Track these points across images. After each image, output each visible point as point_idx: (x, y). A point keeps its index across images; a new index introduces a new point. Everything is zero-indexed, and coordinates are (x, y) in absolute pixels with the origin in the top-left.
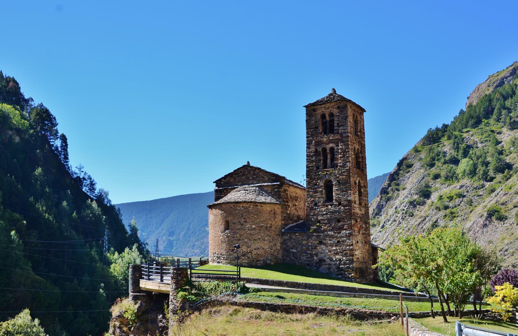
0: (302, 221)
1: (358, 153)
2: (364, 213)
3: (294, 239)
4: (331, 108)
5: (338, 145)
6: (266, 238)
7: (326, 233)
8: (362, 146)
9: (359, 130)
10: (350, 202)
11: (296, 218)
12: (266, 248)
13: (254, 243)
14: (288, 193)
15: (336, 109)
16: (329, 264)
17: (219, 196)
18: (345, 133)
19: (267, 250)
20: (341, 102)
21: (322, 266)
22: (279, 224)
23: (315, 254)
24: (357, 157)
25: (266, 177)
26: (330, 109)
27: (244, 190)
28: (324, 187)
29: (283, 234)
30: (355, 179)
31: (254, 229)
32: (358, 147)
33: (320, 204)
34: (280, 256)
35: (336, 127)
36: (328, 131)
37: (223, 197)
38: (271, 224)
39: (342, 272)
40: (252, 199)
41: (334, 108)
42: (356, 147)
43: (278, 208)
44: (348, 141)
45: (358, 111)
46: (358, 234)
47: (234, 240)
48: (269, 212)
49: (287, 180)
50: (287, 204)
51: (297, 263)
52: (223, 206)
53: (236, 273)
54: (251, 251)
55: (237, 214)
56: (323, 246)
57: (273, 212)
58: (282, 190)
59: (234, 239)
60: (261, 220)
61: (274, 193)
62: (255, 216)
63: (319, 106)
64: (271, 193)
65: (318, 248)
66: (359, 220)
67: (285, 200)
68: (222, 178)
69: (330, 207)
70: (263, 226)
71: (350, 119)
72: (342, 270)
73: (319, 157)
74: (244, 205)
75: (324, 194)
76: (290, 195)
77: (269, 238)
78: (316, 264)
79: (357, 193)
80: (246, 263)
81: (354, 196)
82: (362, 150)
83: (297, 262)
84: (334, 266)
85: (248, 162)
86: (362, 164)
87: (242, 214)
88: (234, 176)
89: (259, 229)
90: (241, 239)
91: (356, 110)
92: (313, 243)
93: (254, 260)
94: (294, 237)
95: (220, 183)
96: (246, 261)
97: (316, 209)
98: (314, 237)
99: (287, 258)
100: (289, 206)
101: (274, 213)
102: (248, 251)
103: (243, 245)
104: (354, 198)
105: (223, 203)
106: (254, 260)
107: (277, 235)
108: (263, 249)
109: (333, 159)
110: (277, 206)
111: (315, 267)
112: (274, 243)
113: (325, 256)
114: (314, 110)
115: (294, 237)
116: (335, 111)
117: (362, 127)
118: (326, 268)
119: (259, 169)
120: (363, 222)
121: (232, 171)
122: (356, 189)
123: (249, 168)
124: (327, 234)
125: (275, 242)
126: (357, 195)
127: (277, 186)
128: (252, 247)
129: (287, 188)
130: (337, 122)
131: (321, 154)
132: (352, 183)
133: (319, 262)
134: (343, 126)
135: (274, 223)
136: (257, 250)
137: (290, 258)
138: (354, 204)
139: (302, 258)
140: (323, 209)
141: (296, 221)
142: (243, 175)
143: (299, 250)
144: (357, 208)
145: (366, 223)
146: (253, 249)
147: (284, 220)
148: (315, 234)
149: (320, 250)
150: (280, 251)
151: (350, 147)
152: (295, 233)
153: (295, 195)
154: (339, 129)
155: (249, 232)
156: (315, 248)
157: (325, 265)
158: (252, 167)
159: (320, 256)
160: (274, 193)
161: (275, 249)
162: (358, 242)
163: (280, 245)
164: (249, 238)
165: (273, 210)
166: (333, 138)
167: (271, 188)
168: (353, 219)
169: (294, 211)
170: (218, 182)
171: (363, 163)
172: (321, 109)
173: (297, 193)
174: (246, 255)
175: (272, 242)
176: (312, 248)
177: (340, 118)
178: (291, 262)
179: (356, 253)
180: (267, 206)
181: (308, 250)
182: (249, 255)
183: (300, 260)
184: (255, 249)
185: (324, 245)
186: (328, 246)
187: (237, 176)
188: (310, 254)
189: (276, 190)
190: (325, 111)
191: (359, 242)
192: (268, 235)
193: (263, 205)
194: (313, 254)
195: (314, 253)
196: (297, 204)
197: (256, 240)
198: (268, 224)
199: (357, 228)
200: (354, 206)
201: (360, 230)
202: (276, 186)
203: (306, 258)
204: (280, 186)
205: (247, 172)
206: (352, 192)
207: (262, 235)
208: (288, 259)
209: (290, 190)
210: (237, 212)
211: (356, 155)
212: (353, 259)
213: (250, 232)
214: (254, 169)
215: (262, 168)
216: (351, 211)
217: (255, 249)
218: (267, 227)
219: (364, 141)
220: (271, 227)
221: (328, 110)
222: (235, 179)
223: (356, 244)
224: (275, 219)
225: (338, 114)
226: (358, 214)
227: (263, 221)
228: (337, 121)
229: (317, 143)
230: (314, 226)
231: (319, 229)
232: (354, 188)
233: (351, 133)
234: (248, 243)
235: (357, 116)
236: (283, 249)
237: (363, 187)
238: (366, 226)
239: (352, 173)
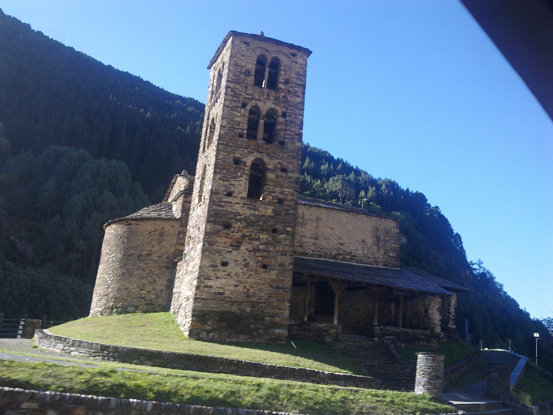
6: (136, 273)
19: (134, 290)
30: (238, 155)
48: (150, 232)
70: (133, 254)
77: (142, 272)
125: (153, 278)
175: (147, 278)
180: (149, 223)
192: (140, 267)
193: (138, 223)
198: (144, 250)
207: (130, 267)
218: (141, 255)
220: (148, 255)
224: (160, 243)
227: (135, 246)
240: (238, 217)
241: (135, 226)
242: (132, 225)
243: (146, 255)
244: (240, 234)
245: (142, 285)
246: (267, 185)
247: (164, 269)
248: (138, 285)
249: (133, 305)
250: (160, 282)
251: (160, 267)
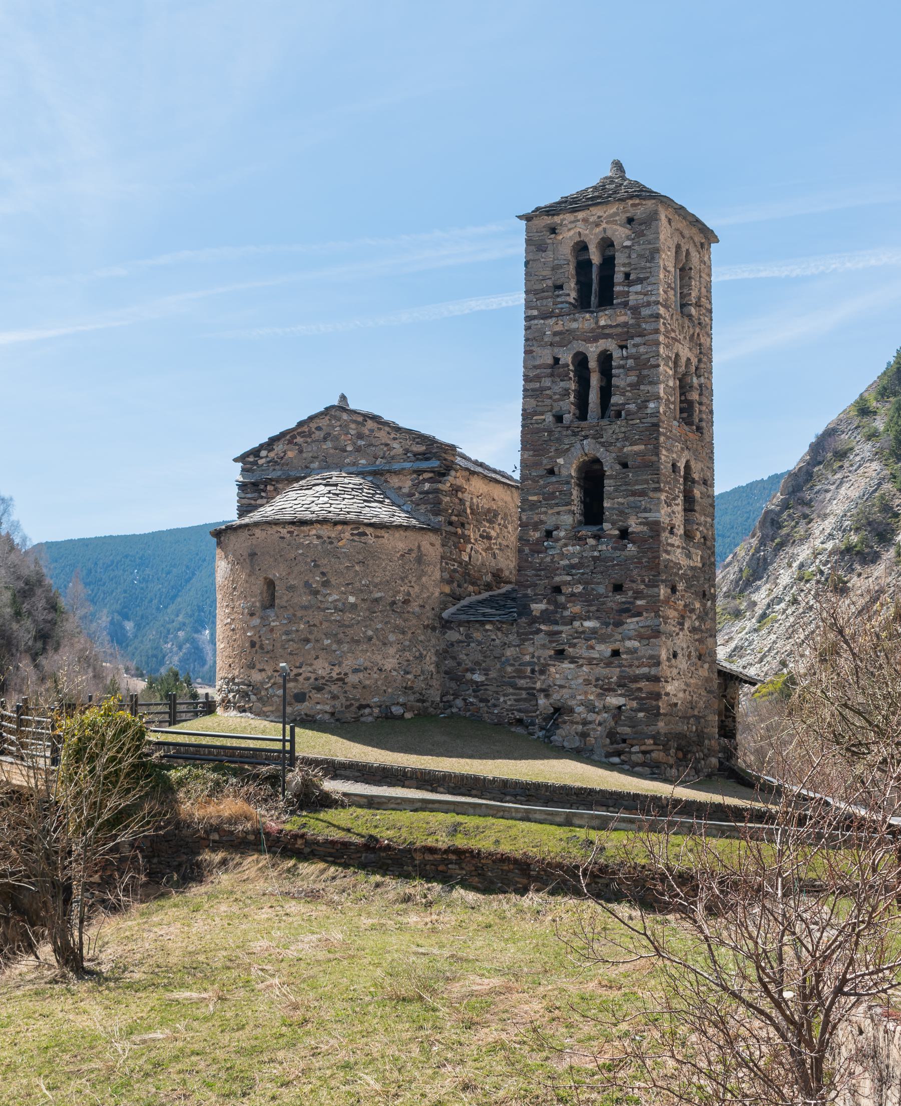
0: (506, 588)
1: (685, 375)
2: (700, 565)
3: (479, 643)
4: (607, 223)
5: (624, 343)
6: (392, 638)
7: (577, 624)
8: (701, 353)
9: (694, 301)
10: (655, 527)
11: (489, 578)
12: (388, 667)
14: (466, 496)
15: (621, 225)
16: (585, 723)
17: (253, 502)
18: (648, 304)
19: (394, 673)
20: (637, 201)
21: (564, 726)
22: (433, 594)
23: (542, 690)
24: (684, 387)
25: (395, 445)
26: (604, 225)
27: (326, 485)
28: (578, 479)
29: (446, 625)
30: (674, 456)
31: (354, 606)
32: (689, 355)
33: (562, 534)
34: (435, 695)
35: (619, 284)
36: (593, 299)
37: (262, 505)
38: (409, 594)
39: (623, 745)
40: (348, 513)
41: (614, 222)
42: (681, 354)
43: (432, 545)
44: (657, 331)
45: (692, 238)
46: (677, 630)
47: (289, 640)
48: (403, 556)
49: (464, 457)
50: (459, 531)
51: (486, 716)
52: (257, 532)
53: (278, 746)
54: (342, 676)
55: (300, 558)
56: (566, 665)
57: (414, 555)
58: (446, 487)
59: (290, 637)
60: (377, 580)
61: (422, 496)
62: (357, 568)
63: (569, 217)
64: (411, 495)
65: (553, 670)
66: (681, 586)
67: (454, 518)
68: (262, 447)
69: (591, 541)
70: (381, 598)
71: (667, 259)
72: (624, 741)
73: (562, 384)
74: (321, 533)
75: (576, 502)
76: (472, 503)
77: (401, 636)
78: (544, 719)
79: (680, 501)
80: (326, 712)
81: (669, 510)
82: (702, 366)
83: (487, 713)
84: (599, 728)
85: (343, 398)
86: (700, 411)
87: (314, 561)
88: (299, 440)
89: (368, 609)
90: (311, 637)
91: (686, 233)
92: (536, 654)
93: (351, 705)
94: (477, 635)
95: (255, 463)
96: (327, 708)
97: (547, 548)
98: (542, 635)
99: (454, 699)
100: (467, 540)
101: (419, 560)
102: (334, 675)
103: (317, 657)
104: (669, 516)
105: (256, 524)
106: (351, 705)
107: (426, 627)
108: (381, 670)
109: (606, 392)
110: (427, 537)
111: (542, 728)
112: (417, 654)
113: (573, 697)
114: (553, 230)
115: (477, 635)
116: (620, 234)
117: (703, 290)
118: (573, 733)
119: (375, 418)
120: (696, 593)
121: (293, 425)
122: (675, 486)
123: (345, 416)
124: (581, 629)
126: (679, 509)
127: (431, 475)
129: (460, 482)
130: (622, 269)
131: (572, 375)
132: (665, 468)
133: (554, 714)
134: (641, 283)
135: (417, 589)
136: (361, 675)
137: (465, 700)
138: (667, 534)
139: (502, 699)
140: (570, 548)
141: (488, 587)
142: (325, 439)
143: (493, 674)
144: (678, 547)
145: (704, 595)
146: (349, 671)
147: (450, 582)
148: (543, 627)
149: (557, 676)
150: (434, 677)
151: (661, 351)
152: (483, 623)
153: (486, 506)
154: (628, 292)
155: (336, 617)
156: (542, 672)
157: (572, 722)
158: (355, 412)
159: (556, 696)
160: (422, 496)
161: (419, 672)
162: (675, 655)
163: (434, 658)
164: (336, 635)
165: (415, 548)
166: (610, 323)
167: (412, 480)
168: (663, 581)
169: (484, 554)
170: (249, 459)
171: (704, 408)
172: (573, 225)
173: (494, 500)
176: (533, 671)
177: (634, 256)
178: (468, 714)
179: (670, 688)
180: (397, 535)
181: (520, 677)
183: (495, 706)
184: (356, 671)
185: (570, 663)
186: (582, 666)
187: (309, 440)
188: (525, 689)
189: (427, 486)
190: (587, 232)
191: (680, 656)
192: (397, 627)
193: (382, 532)
194: (534, 689)
195: (538, 685)
196: (493, 534)
197: (358, 642)
198: (399, 592)
199: (676, 610)
200: (669, 541)
201: (683, 617)
202: (427, 475)
203: (515, 700)
204: (441, 474)
205: (338, 429)
206: (663, 497)
207: (379, 626)
208: (459, 702)
209: (472, 489)
210: (300, 551)
211: (680, 380)
212: (658, 708)
213: (338, 618)
214: (360, 419)
215: (387, 417)
216: (658, 557)
217: (356, 671)
219: (709, 336)
220: (406, 602)
221: (597, 230)
222: (301, 452)
223: (669, 660)
224: (419, 578)
225: (628, 243)
226: (681, 568)
227: (381, 583)
228: (624, 265)
229: (557, 339)
230: (541, 602)
231: (557, 612)
232: (669, 483)
233: (666, 307)
234: (335, 651)
235: (688, 253)
236: (446, 673)
237: (699, 484)
238: (704, 605)
239: (664, 435)
240: (680, 572)
241: (373, 539)
242: (367, 535)
243: (403, 603)
244: (683, 603)
245: (405, 663)
246: (695, 511)
247: (429, 631)
248: (399, 663)
249: (398, 703)
250: (428, 658)
251: (424, 626)
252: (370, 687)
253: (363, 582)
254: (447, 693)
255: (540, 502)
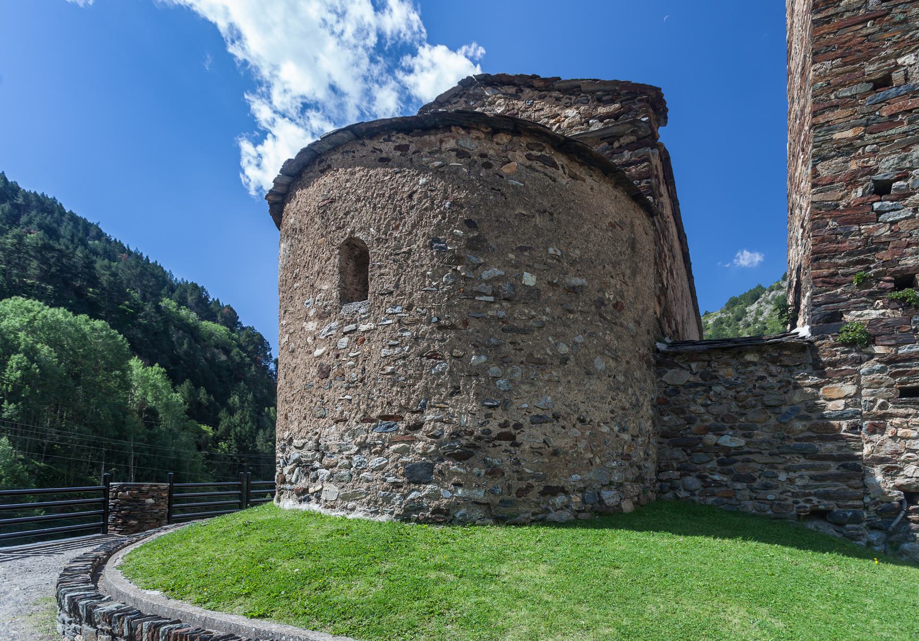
13: (532, 384)
102: (494, 427)
108: (582, 421)
128: (517, 403)
136: (548, 427)
164: (497, 346)
174: (480, 454)
182: (499, 456)
197: (540, 364)
208: (692, 481)
213: (502, 314)
217: (538, 420)
234: (495, 378)
252: (566, 453)
253: (551, 251)
254: (668, 467)
255: (861, 138)
